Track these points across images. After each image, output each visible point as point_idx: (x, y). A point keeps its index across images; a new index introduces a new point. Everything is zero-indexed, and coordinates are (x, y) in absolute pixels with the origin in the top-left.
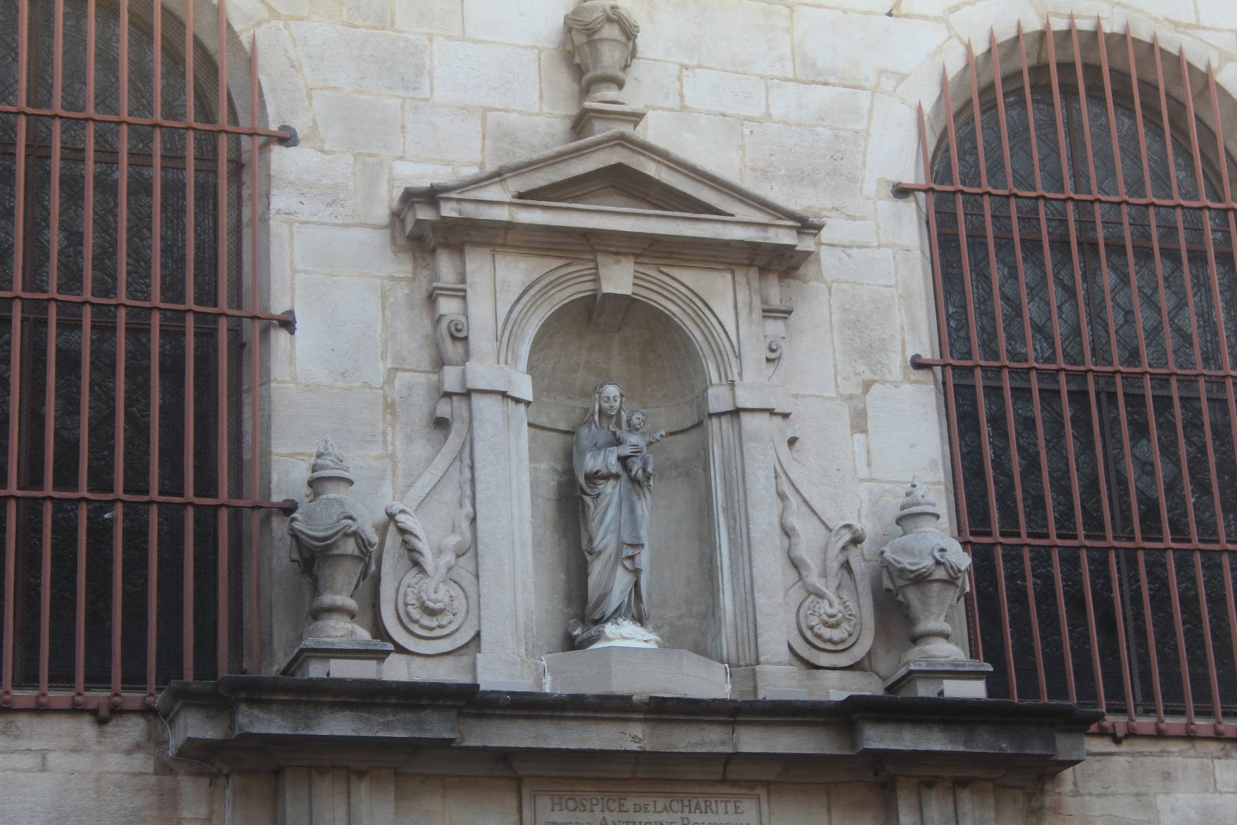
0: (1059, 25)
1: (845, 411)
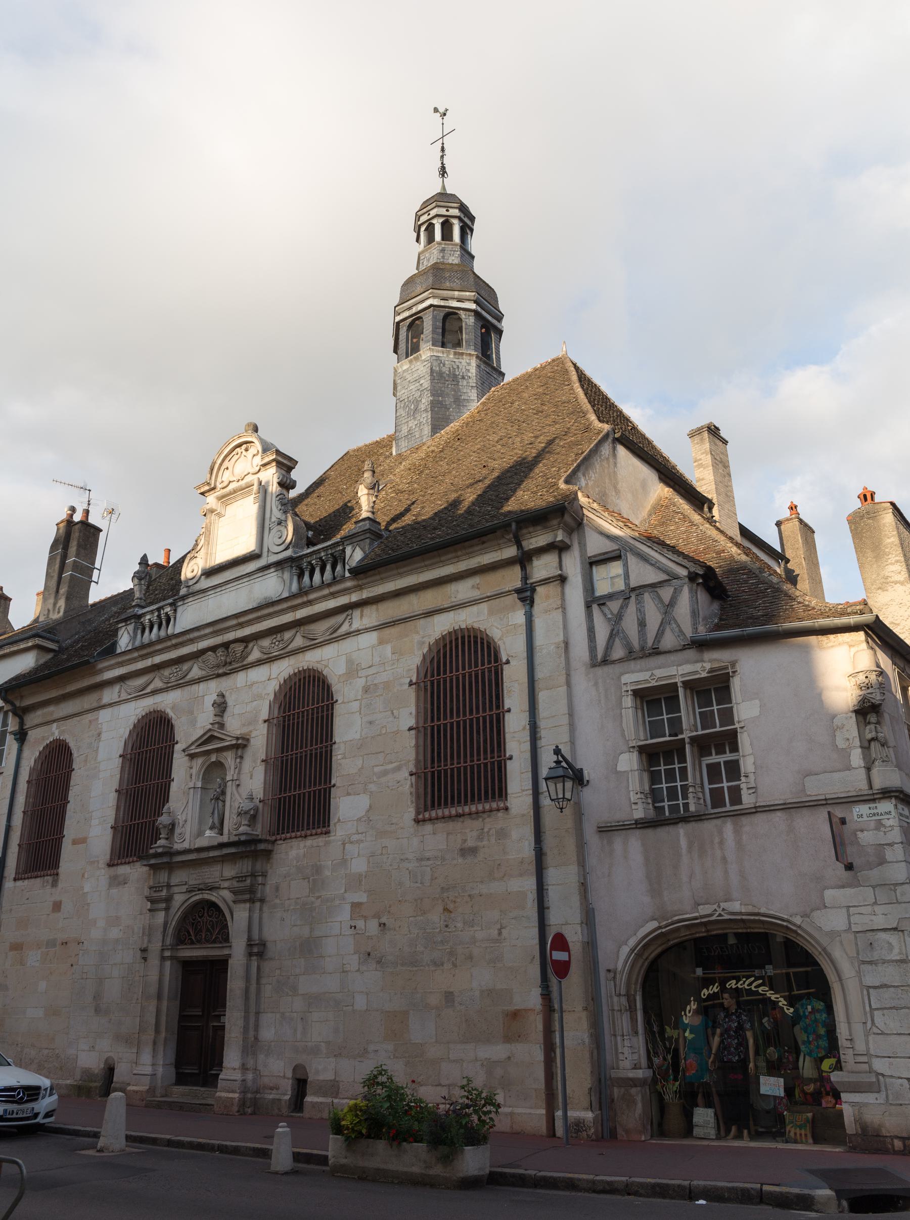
0: (296, 671)
1: (249, 775)
